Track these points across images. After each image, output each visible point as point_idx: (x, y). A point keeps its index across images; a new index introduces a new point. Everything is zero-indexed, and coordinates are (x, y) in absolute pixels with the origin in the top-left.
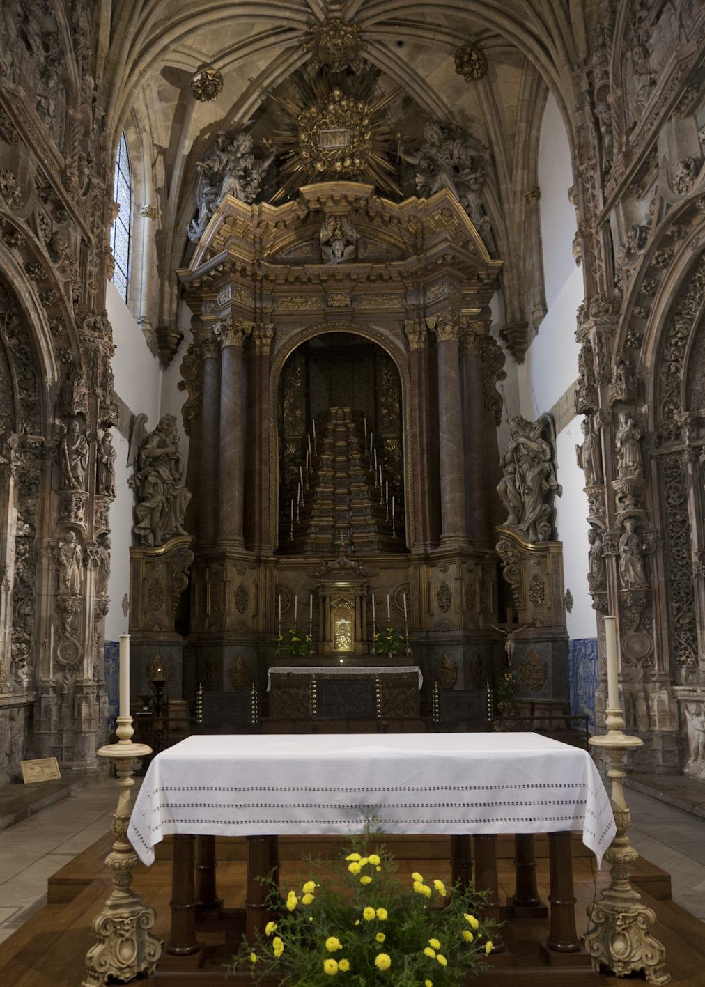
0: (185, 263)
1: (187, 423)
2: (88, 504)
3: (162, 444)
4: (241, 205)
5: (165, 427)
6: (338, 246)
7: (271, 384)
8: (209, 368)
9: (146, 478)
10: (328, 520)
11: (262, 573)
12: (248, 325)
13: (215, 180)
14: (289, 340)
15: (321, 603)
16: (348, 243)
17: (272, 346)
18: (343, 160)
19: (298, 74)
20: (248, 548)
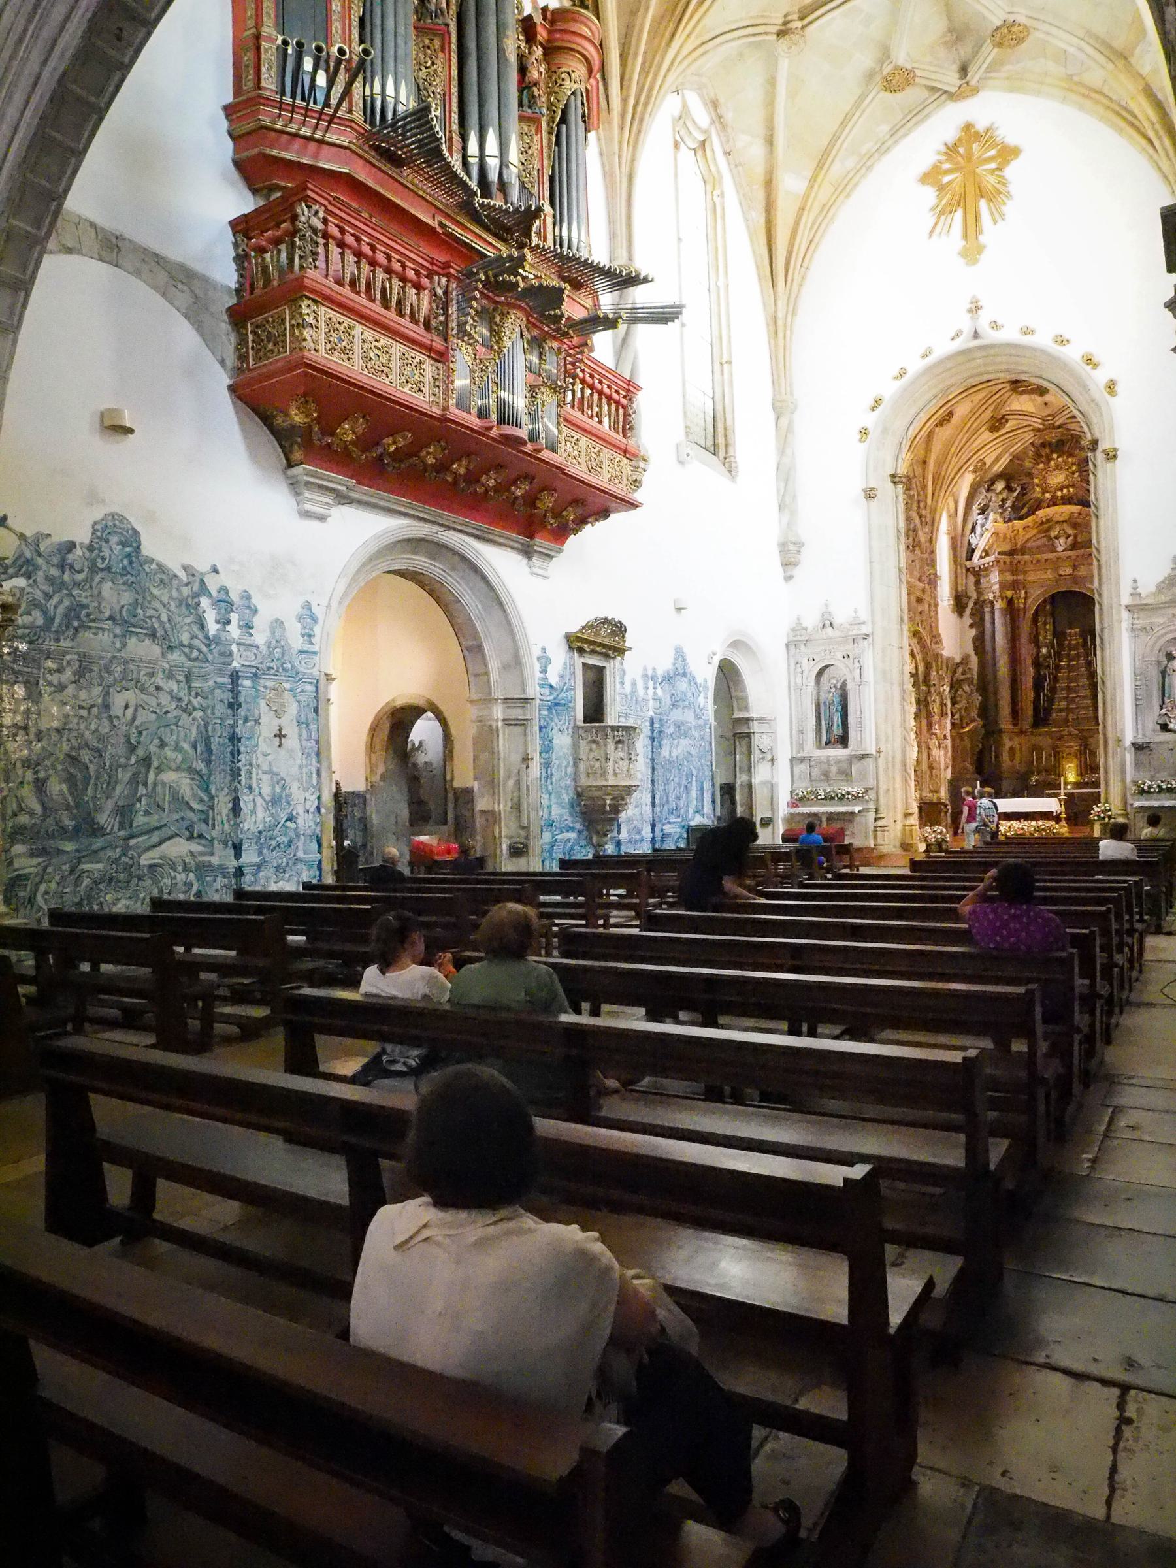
0: (969, 558)
1: (976, 649)
2: (939, 722)
3: (964, 673)
4: (1002, 527)
5: (965, 660)
6: (1062, 540)
7: (1025, 627)
8: (987, 617)
9: (956, 691)
10: (1063, 704)
11: (1023, 739)
12: (1009, 593)
13: (983, 511)
14: (1034, 596)
15: (1057, 754)
16: (1069, 536)
17: (1025, 604)
18: (1061, 490)
19: (1032, 444)
20: (1015, 725)
